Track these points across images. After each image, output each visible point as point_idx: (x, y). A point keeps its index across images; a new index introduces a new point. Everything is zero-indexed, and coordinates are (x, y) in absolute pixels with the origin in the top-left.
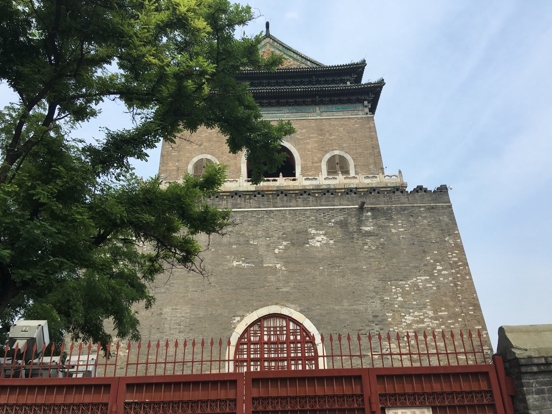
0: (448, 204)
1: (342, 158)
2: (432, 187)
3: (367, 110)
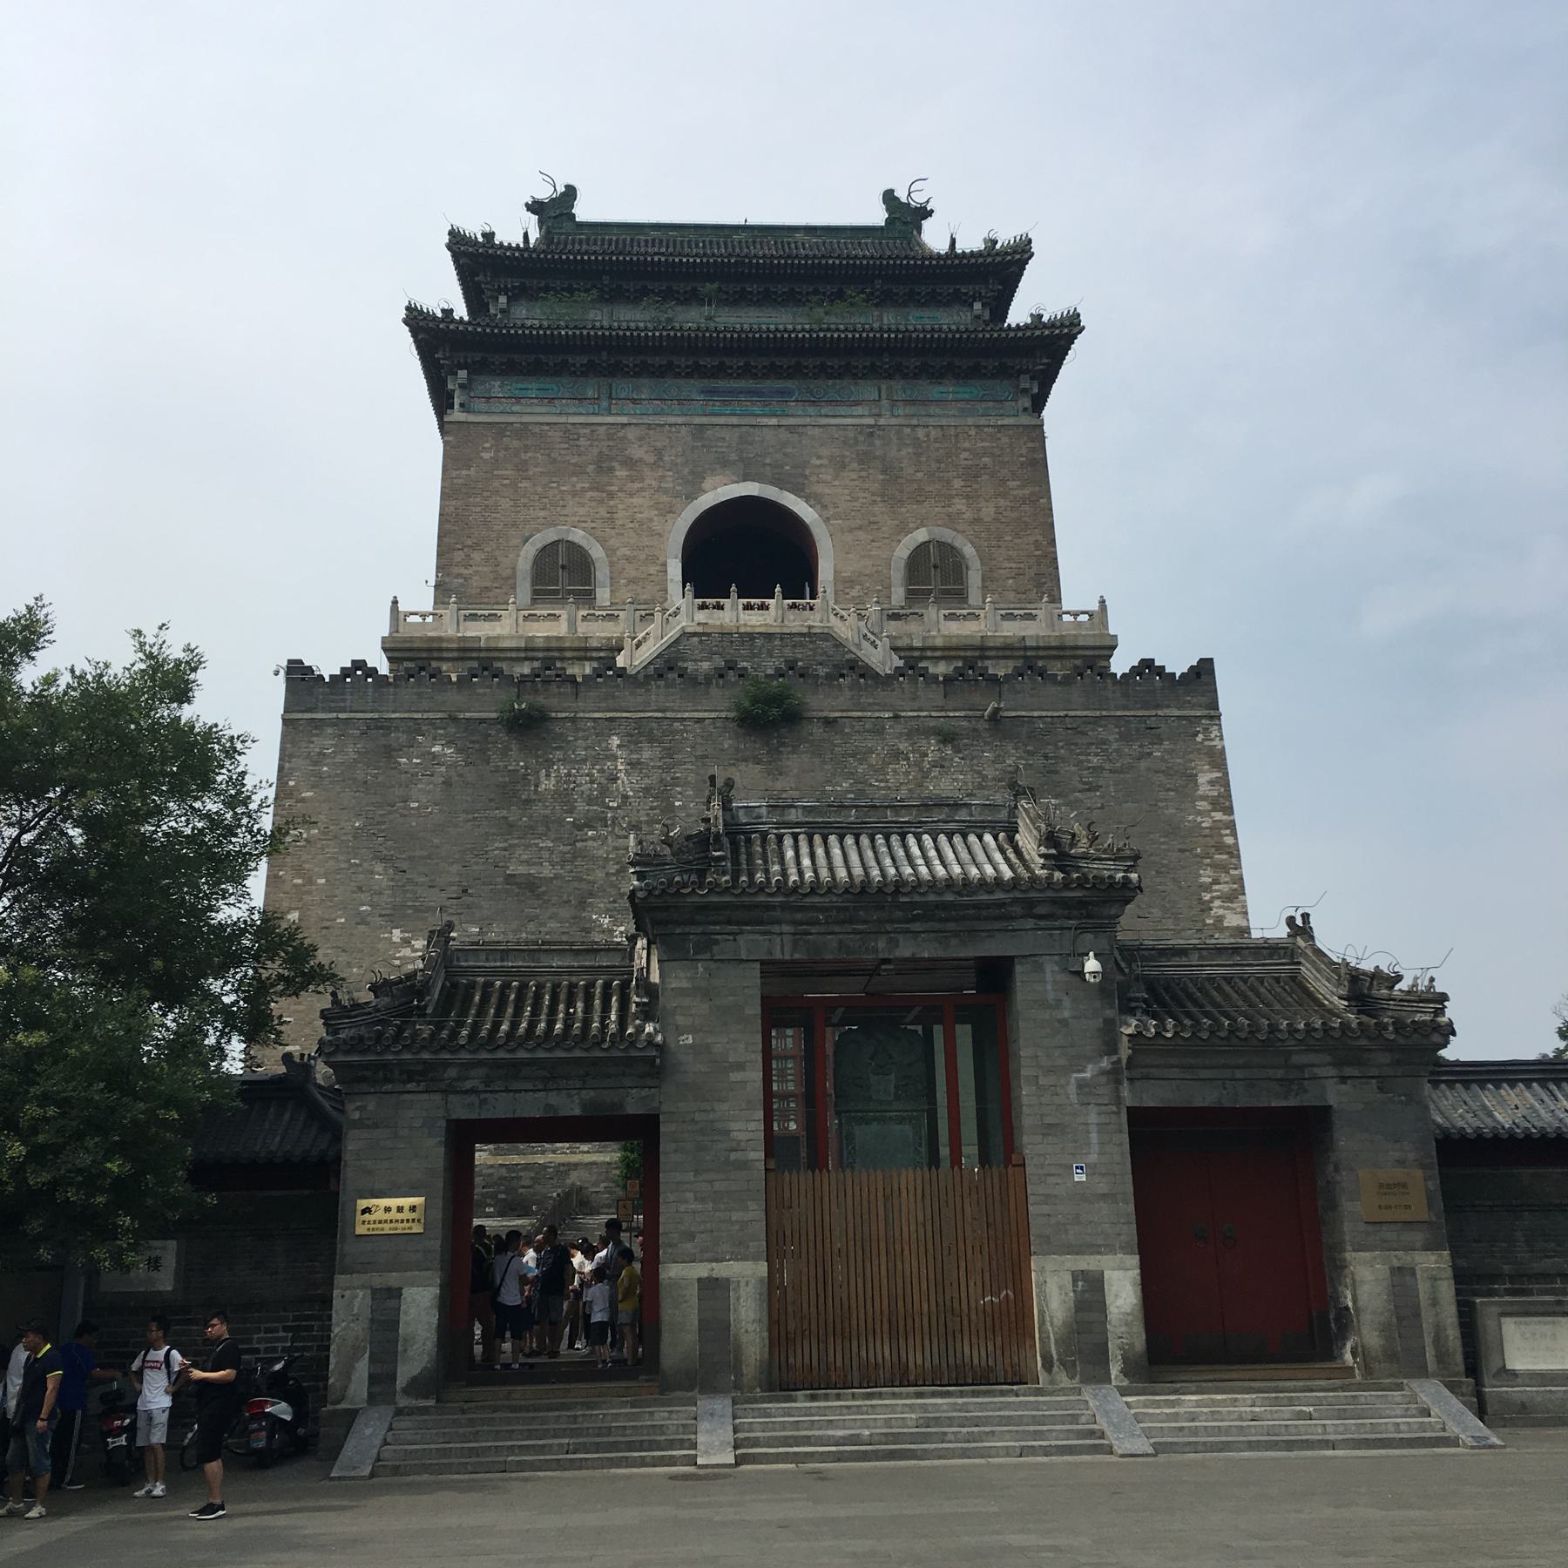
0: (1213, 713)
1: (947, 550)
2: (1178, 665)
3: (1027, 402)
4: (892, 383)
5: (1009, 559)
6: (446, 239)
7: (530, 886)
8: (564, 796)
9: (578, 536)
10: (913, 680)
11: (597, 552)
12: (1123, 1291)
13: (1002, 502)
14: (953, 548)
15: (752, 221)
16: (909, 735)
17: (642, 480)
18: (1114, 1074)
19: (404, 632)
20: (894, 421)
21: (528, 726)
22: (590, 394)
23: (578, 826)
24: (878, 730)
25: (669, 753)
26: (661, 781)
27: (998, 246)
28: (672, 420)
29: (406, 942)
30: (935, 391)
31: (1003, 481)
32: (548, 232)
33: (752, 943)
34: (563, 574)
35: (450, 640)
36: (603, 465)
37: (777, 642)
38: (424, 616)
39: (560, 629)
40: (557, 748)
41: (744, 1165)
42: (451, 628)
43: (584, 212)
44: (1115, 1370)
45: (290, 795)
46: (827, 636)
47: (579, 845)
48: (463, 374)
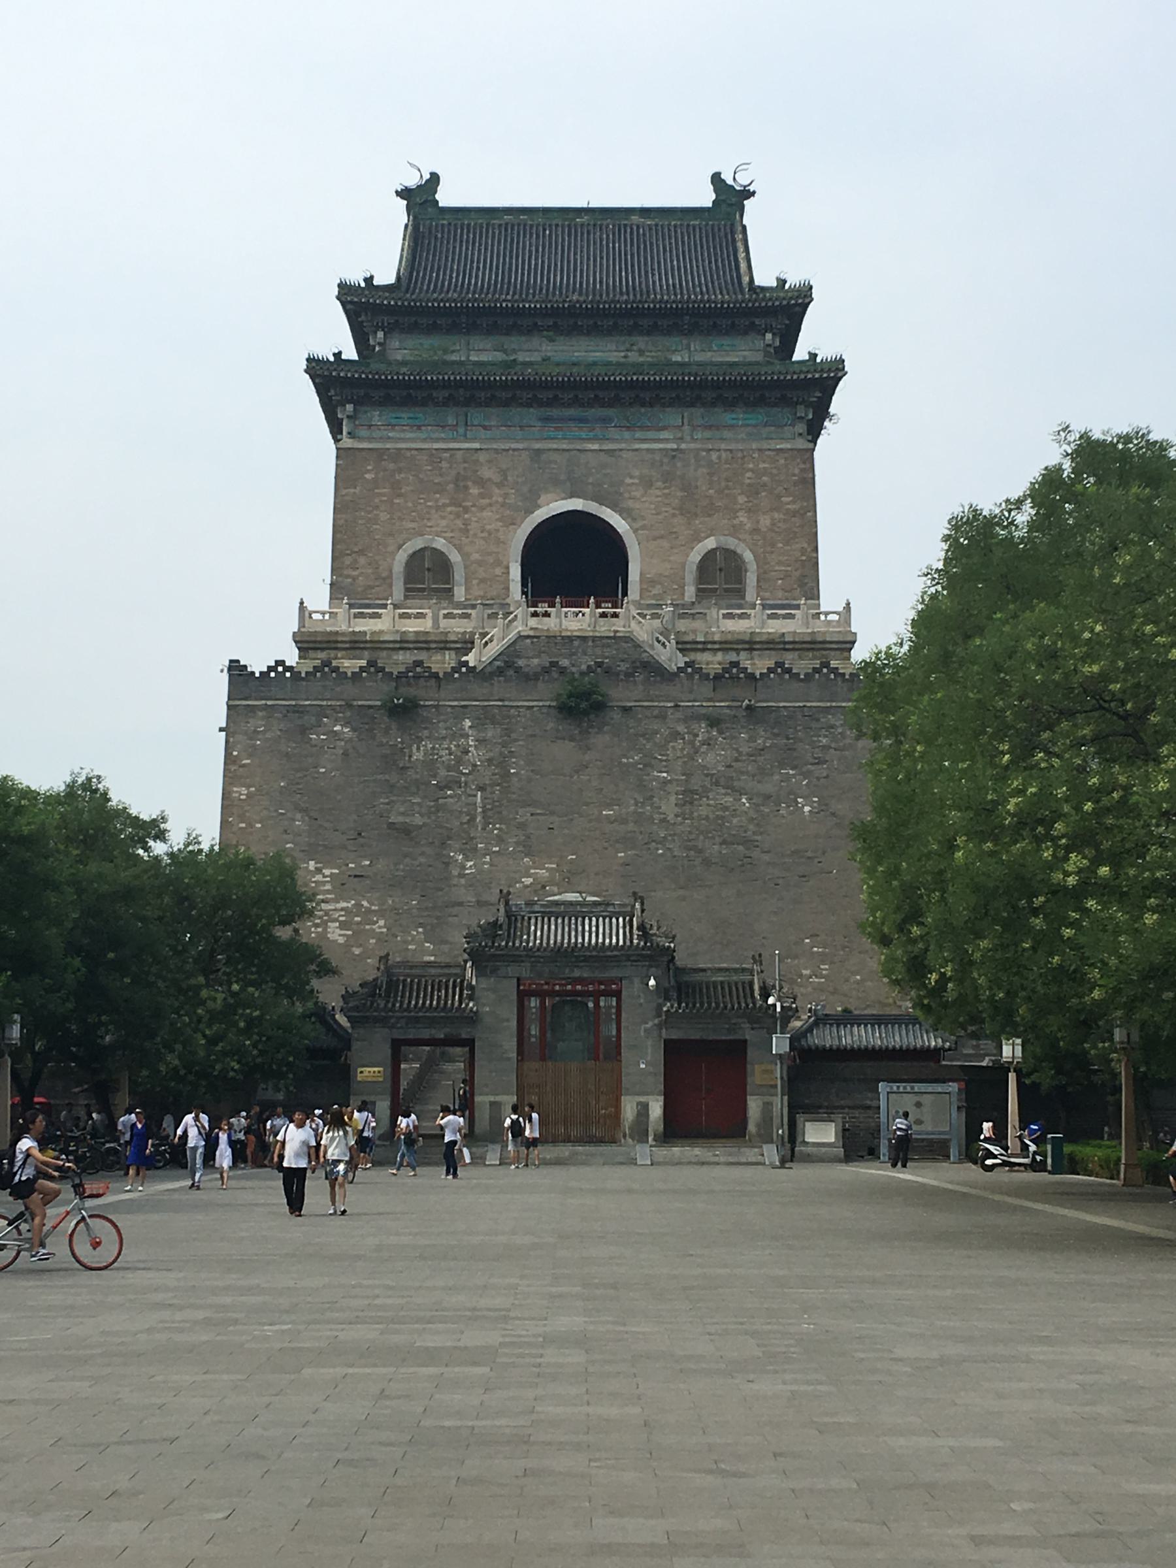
1: (731, 555)
3: (801, 428)
4: (693, 410)
5: (779, 563)
6: (336, 291)
7: (406, 831)
8: (431, 765)
9: (440, 543)
10: (690, 677)
11: (455, 557)
12: (656, 1109)
13: (776, 515)
14: (735, 553)
15: (594, 204)
16: (685, 720)
17: (491, 497)
18: (659, 1026)
19: (310, 627)
20: (692, 446)
21: (404, 712)
22: (450, 422)
23: (441, 787)
24: (662, 716)
25: (508, 732)
26: (501, 753)
27: (787, 287)
28: (513, 446)
29: (319, 871)
30: (728, 418)
31: (779, 497)
32: (415, 218)
33: (513, 970)
34: (429, 575)
35: (343, 634)
36: (460, 483)
37: (590, 643)
38: (323, 613)
39: (426, 625)
40: (425, 728)
41: (509, 1059)
42: (346, 624)
43: (446, 197)
44: (650, 1139)
45: (234, 762)
46: (628, 639)
47: (441, 801)
48: (350, 407)
